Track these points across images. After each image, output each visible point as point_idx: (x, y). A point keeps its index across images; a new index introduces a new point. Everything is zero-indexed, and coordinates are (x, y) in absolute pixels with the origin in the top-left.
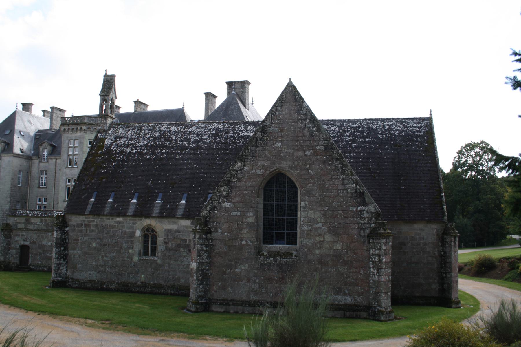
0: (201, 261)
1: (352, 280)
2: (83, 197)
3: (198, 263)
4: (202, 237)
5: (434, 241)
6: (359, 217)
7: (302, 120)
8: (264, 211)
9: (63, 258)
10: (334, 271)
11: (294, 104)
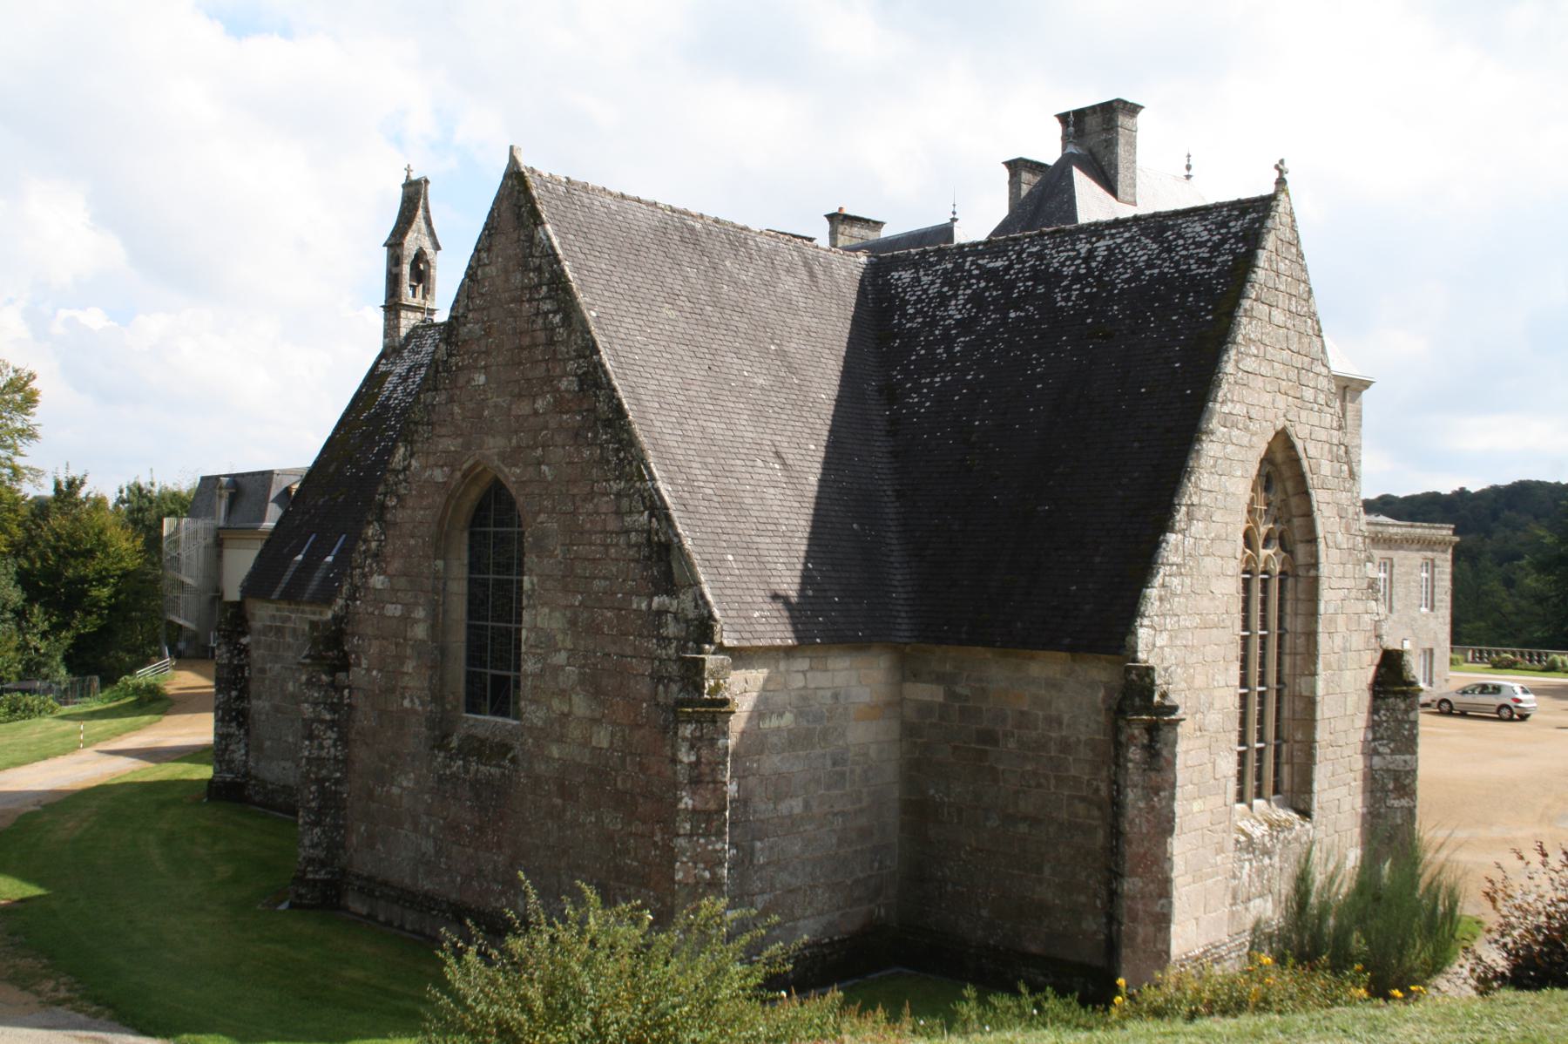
0: (315, 753)
1: (635, 864)
2: (285, 551)
3: (308, 759)
4: (319, 680)
5: (1097, 737)
6: (653, 637)
7: (531, 289)
8: (470, 603)
9: (236, 718)
10: (591, 822)
11: (515, 236)
